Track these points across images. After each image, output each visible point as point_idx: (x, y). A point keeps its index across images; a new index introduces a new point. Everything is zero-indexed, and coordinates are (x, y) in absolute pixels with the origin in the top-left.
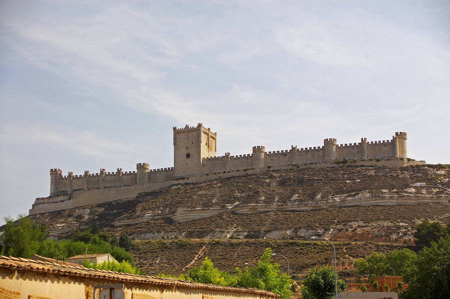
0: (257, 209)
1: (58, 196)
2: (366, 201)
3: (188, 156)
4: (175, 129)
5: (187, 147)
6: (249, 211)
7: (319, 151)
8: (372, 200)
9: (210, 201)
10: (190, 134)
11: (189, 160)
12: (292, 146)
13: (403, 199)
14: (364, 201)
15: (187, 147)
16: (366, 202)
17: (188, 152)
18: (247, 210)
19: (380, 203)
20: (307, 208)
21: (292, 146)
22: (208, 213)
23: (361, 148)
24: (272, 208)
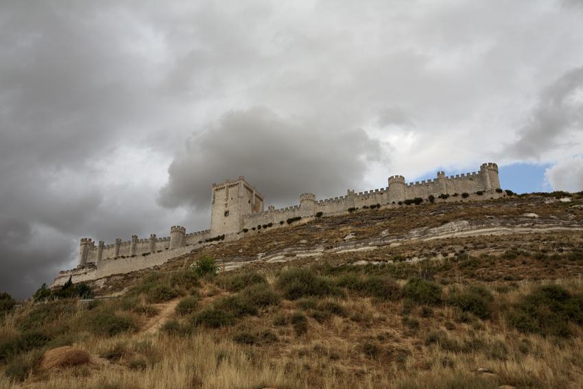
0: (295, 255)
1: (83, 268)
2: (462, 231)
3: (226, 213)
4: (214, 185)
5: (226, 205)
6: (283, 259)
7: (382, 194)
8: (472, 229)
9: (237, 251)
10: (230, 189)
11: (227, 218)
12: (348, 190)
13: (522, 227)
14: (458, 231)
15: (226, 205)
16: (460, 233)
17: (227, 209)
18: (281, 257)
19: (486, 232)
20: (368, 248)
21: (348, 190)
22: (231, 265)
23: (438, 185)
24: (317, 252)
